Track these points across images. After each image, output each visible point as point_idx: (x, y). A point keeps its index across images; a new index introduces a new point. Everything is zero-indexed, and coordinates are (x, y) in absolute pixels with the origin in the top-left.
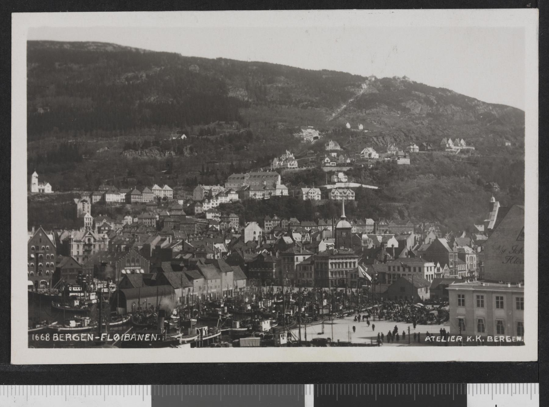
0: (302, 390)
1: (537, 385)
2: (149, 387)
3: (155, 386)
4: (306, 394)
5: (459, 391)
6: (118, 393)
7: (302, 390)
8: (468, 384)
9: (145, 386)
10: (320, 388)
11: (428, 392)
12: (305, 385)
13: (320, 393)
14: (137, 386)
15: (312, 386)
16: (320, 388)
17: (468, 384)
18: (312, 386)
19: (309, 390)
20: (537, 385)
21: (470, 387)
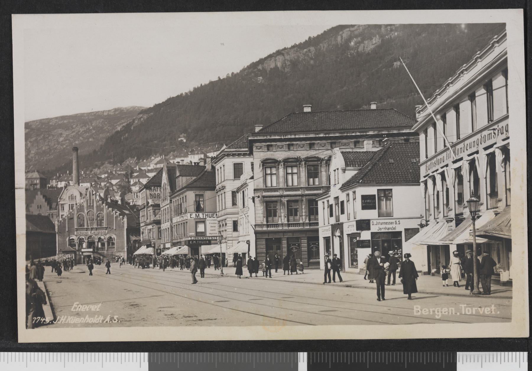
0: (296, 358)
1: (526, 354)
2: (146, 354)
3: (152, 353)
4: (300, 362)
5: (450, 360)
7: (296, 358)
8: (458, 353)
9: (142, 353)
10: (313, 356)
12: (299, 353)
13: (313, 360)
14: (135, 353)
15: (306, 354)
16: (313, 356)
17: (458, 353)
18: (306, 354)
19: (303, 358)
20: (526, 354)
21: (460, 355)
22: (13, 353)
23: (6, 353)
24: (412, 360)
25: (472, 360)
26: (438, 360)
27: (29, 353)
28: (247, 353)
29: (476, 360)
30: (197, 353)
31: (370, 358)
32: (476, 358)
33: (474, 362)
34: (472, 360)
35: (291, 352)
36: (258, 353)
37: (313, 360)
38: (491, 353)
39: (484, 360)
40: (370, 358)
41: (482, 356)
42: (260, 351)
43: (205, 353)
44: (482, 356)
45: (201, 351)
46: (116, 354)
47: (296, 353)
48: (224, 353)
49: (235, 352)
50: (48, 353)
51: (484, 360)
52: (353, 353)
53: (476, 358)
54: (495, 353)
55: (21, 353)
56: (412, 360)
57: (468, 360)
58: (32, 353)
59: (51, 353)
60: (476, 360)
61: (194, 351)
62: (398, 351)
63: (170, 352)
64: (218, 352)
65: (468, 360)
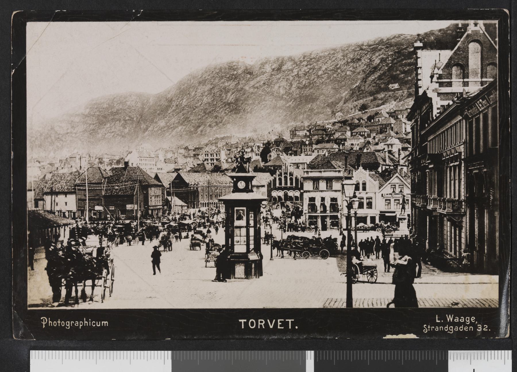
1: (510, 352)
3: (175, 352)
6: (57, 357)
8: (449, 351)
9: (166, 352)
10: (319, 354)
11: (363, 358)
13: (319, 357)
15: (313, 352)
16: (319, 354)
17: (449, 351)
18: (313, 352)
19: (310, 356)
20: (510, 352)
22: (51, 351)
23: (44, 351)
24: (408, 358)
25: (462, 358)
26: (414, 357)
27: (64, 351)
28: (260, 351)
29: (466, 358)
30: (215, 351)
31: (370, 355)
32: (466, 356)
33: (464, 359)
34: (462, 358)
35: (300, 350)
36: (270, 351)
37: (319, 357)
38: (479, 352)
39: (472, 357)
40: (370, 355)
41: (471, 354)
42: (271, 350)
43: (222, 351)
44: (471, 354)
45: (218, 350)
46: (142, 352)
47: (304, 351)
48: (239, 352)
49: (249, 350)
50: (81, 352)
51: (472, 357)
52: (355, 351)
53: (466, 356)
54: (482, 351)
55: (57, 351)
56: (408, 358)
57: (459, 358)
58: (67, 352)
59: (85, 352)
60: (466, 358)
61: (213, 350)
62: (395, 349)
63: (191, 350)
64: (234, 350)
65: (459, 358)
